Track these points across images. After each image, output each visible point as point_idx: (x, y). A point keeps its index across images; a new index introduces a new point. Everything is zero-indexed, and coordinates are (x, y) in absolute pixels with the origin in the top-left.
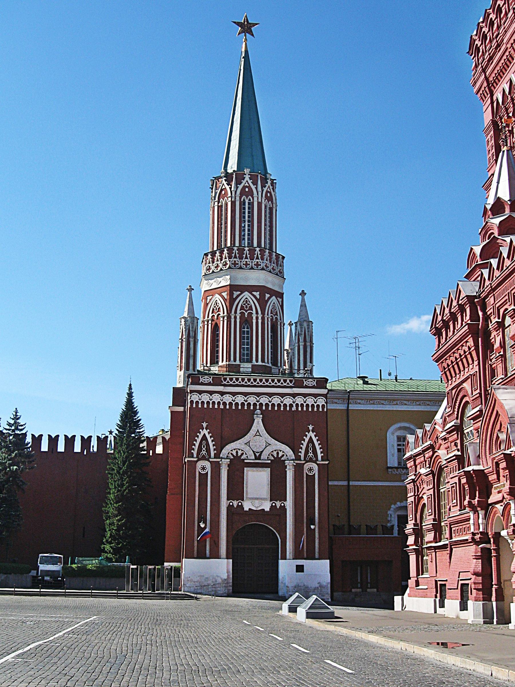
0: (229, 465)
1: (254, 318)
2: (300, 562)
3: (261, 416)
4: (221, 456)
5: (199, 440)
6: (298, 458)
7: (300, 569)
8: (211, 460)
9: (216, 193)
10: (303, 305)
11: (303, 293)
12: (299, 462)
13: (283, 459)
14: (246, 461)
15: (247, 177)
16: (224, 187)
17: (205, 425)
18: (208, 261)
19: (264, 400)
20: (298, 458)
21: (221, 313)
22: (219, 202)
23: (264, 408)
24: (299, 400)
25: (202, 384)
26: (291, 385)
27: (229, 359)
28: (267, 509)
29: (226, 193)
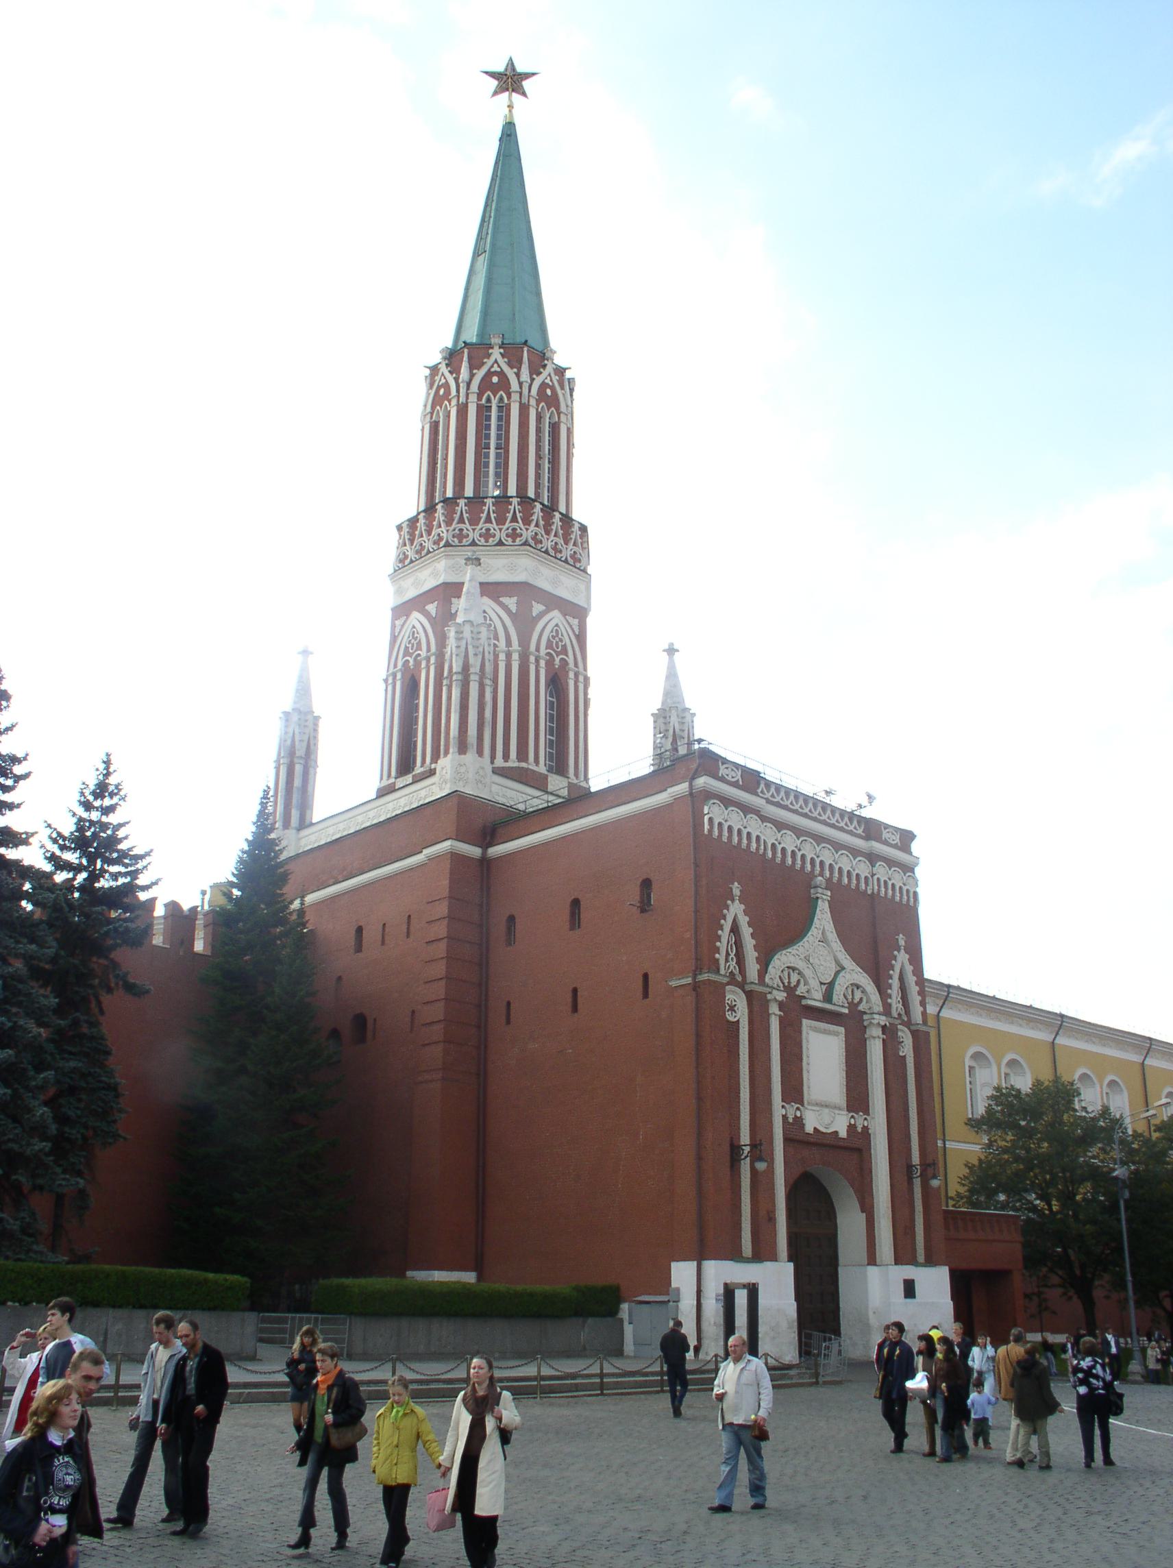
0: (781, 1005)
1: (571, 675)
2: (909, 1272)
3: (829, 893)
4: (767, 980)
5: (727, 925)
6: (887, 1010)
7: (909, 1289)
8: (748, 988)
9: (472, 376)
10: (672, 675)
11: (671, 651)
12: (892, 1021)
13: (861, 1008)
14: (804, 1002)
15: (549, 369)
16: (496, 368)
17: (736, 889)
18: (457, 517)
19: (827, 856)
20: (887, 1010)
21: (502, 644)
22: (480, 397)
23: (827, 874)
24: (881, 871)
25: (722, 779)
26: (860, 831)
27: (522, 756)
28: (843, 1134)
29: (504, 384)
